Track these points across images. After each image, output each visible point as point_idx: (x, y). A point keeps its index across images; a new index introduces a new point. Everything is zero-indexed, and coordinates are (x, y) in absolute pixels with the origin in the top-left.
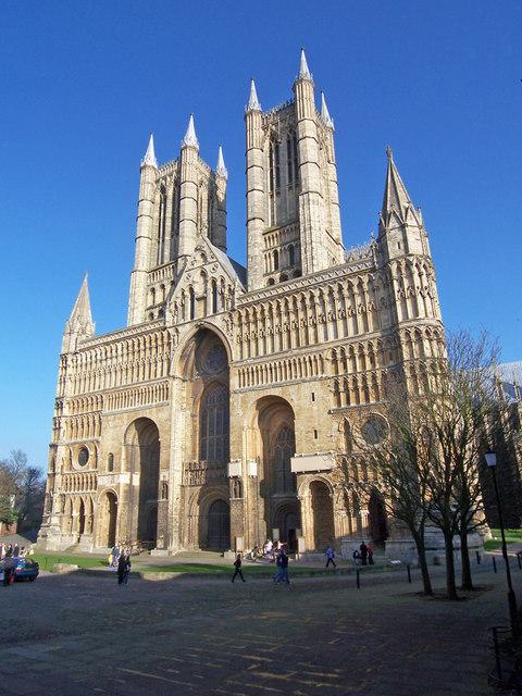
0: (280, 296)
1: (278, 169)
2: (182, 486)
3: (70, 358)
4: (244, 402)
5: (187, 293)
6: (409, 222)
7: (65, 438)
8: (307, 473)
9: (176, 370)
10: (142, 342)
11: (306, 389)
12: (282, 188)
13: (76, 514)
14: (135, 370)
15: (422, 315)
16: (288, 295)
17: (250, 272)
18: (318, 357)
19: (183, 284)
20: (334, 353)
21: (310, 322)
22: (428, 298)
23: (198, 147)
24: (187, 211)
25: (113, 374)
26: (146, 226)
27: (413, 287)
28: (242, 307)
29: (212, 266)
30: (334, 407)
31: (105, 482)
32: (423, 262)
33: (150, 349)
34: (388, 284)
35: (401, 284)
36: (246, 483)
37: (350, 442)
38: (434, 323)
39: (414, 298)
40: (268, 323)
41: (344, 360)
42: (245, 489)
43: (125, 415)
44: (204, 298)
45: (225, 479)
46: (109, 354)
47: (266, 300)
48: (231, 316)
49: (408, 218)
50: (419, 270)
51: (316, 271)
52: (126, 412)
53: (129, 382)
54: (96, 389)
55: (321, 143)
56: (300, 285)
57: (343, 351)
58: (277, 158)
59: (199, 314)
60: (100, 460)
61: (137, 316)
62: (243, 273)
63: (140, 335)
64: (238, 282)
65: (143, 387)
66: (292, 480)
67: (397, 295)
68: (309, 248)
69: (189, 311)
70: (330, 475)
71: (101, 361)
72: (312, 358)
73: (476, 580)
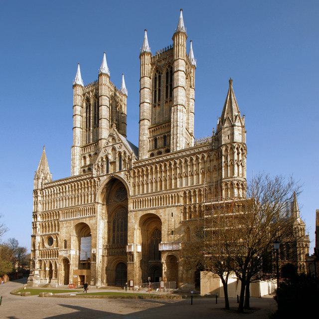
0: (157, 163)
1: (159, 90)
2: (103, 256)
3: (39, 192)
4: (136, 216)
5: (104, 159)
6: (237, 124)
7: (39, 232)
8: (167, 251)
9: (99, 199)
10: (80, 184)
12: (161, 102)
13: (47, 269)
14: (77, 199)
15: (236, 175)
16: (162, 162)
17: (141, 149)
18: (176, 195)
19: (102, 154)
20: (185, 193)
21: (173, 177)
22: (240, 167)
25: (64, 201)
28: (135, 168)
29: (119, 145)
30: (182, 220)
31: (63, 254)
34: (219, 158)
36: (135, 255)
37: (189, 237)
38: (242, 180)
39: (233, 165)
40: (150, 177)
41: (190, 196)
42: (135, 258)
44: (114, 163)
46: (61, 191)
47: (148, 165)
48: (129, 172)
49: (237, 121)
51: (178, 149)
53: (73, 205)
54: (55, 208)
55: (187, 74)
56: (168, 157)
57: (190, 192)
58: (160, 83)
59: (111, 171)
60: (59, 243)
61: (77, 171)
62: (136, 150)
63: (79, 181)
64: (133, 155)
65: (81, 208)
66: (160, 254)
68: (175, 137)
69: (106, 168)
71: (57, 193)
73: (251, 304)
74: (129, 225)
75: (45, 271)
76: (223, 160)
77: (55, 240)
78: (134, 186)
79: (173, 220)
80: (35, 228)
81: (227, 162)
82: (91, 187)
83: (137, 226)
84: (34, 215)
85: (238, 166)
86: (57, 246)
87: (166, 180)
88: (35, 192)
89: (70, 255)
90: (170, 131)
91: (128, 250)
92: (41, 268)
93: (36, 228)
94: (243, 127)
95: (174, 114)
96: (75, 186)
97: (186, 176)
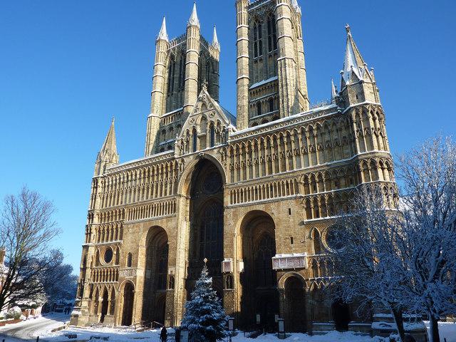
3: (100, 180)
4: (235, 215)
5: (191, 133)
9: (183, 189)
11: (284, 207)
13: (101, 299)
16: (271, 135)
20: (306, 179)
21: (287, 155)
22: (380, 137)
23: (199, 26)
24: (191, 73)
26: (160, 83)
27: (369, 128)
28: (234, 143)
29: (211, 112)
31: (124, 274)
32: (376, 109)
33: (162, 174)
35: (359, 126)
39: (369, 135)
42: (235, 283)
43: (142, 224)
44: (205, 136)
45: (221, 274)
46: (130, 178)
48: (224, 150)
50: (373, 115)
52: (143, 221)
57: (313, 177)
60: (121, 258)
67: (356, 135)
68: (285, 99)
70: (303, 271)
71: (123, 182)
72: (289, 182)
74: (226, 228)
75: (97, 301)
76: (355, 129)
77: (115, 253)
78: (232, 170)
79: (291, 220)
80: (89, 234)
81: (361, 130)
82: (171, 172)
83: (237, 230)
84: (89, 215)
85: (377, 136)
86: (117, 263)
87: (277, 160)
88: (95, 181)
89: (136, 276)
90: (278, 92)
91: (224, 270)
92: (91, 297)
93: (91, 233)
94: (373, 84)
95: (281, 70)
96: (149, 171)
97: (306, 154)
